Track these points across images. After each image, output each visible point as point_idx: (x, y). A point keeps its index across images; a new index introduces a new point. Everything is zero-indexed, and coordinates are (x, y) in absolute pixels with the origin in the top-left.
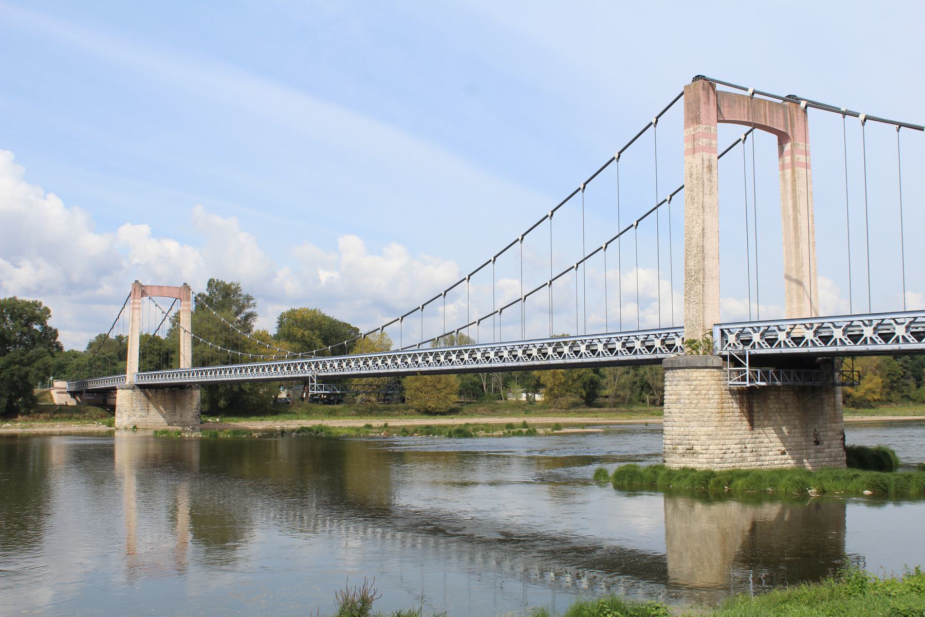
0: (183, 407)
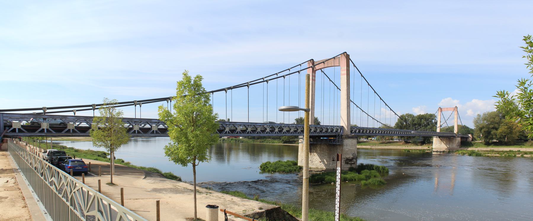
0: (453, 143)
